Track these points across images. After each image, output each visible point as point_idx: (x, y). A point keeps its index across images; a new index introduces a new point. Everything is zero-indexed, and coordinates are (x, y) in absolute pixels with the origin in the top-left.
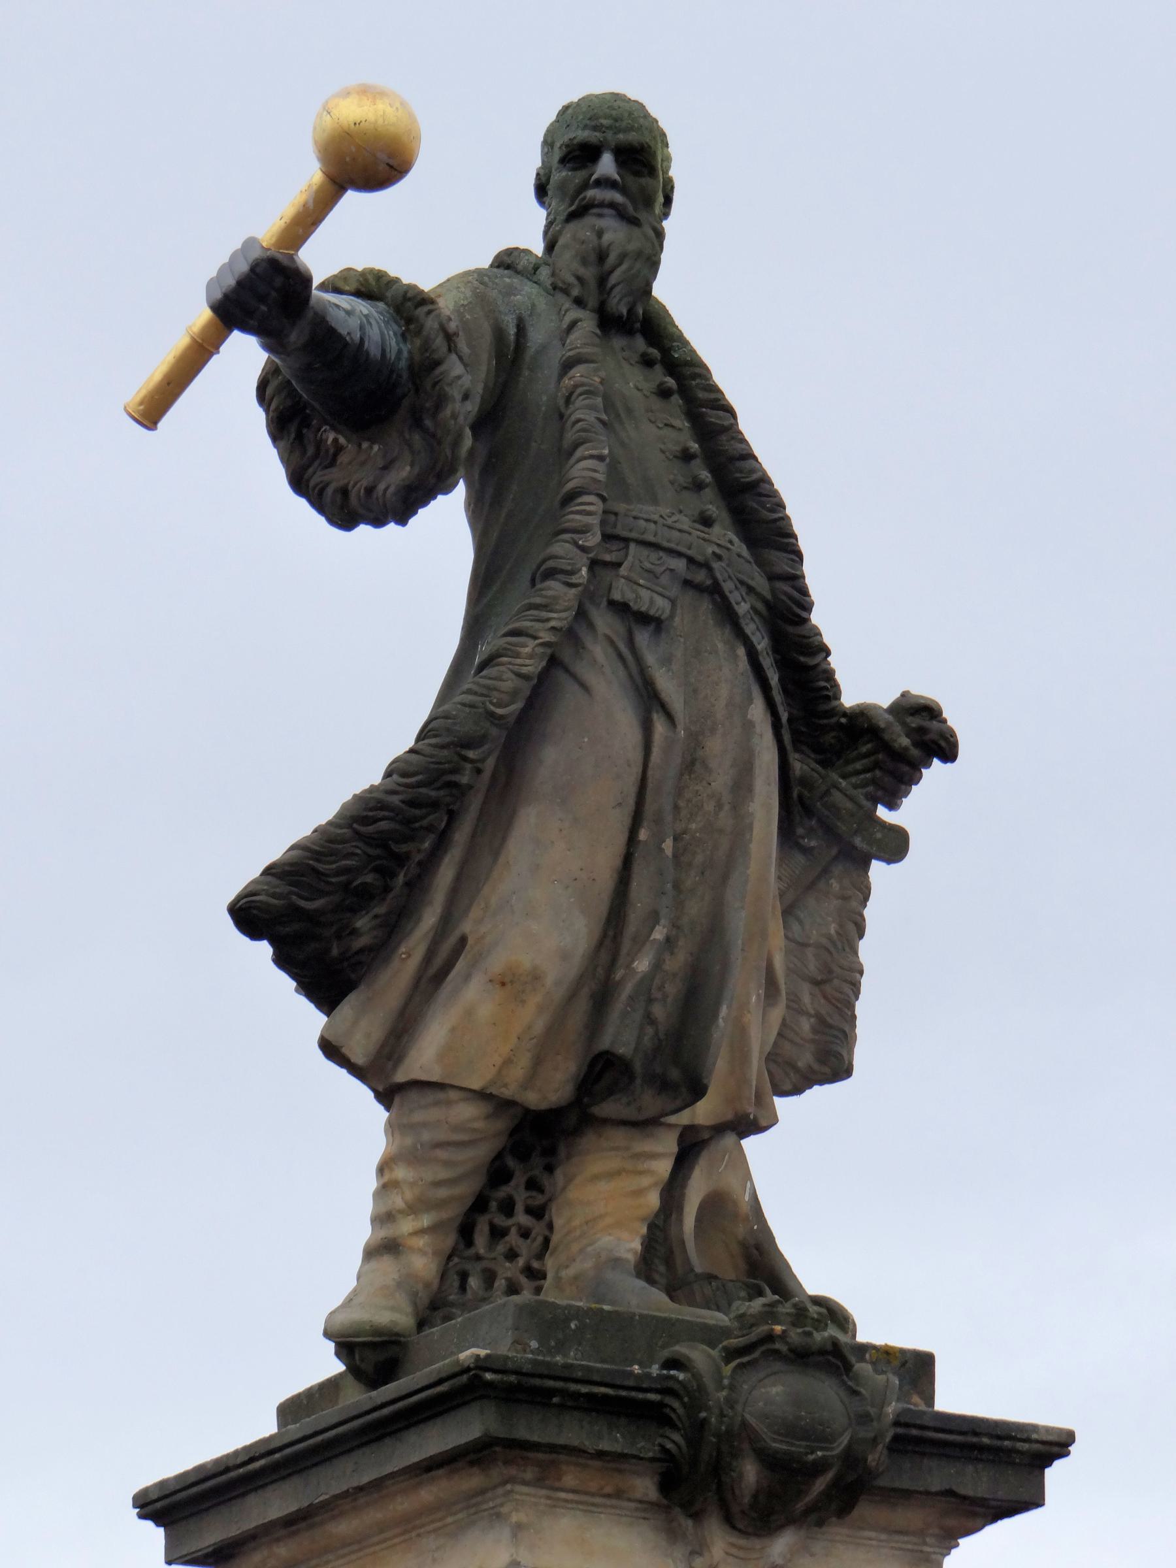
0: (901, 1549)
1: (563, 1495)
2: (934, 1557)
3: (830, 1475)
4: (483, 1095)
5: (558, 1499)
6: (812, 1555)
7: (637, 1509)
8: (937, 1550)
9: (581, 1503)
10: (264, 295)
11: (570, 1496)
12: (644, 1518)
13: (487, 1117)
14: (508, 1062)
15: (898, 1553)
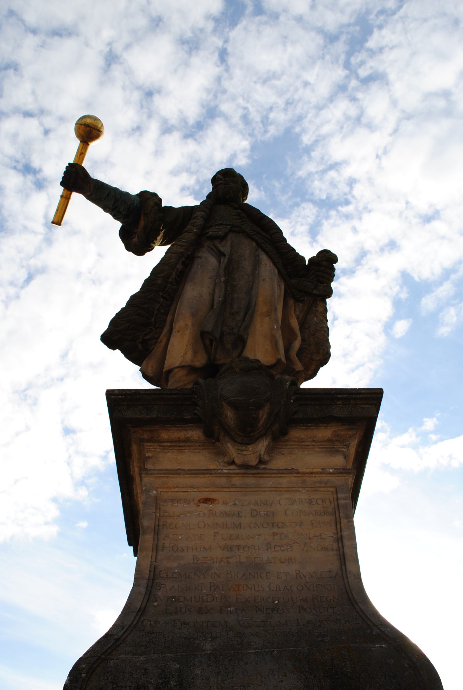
0: (324, 448)
1: (165, 444)
2: (341, 450)
3: (267, 409)
4: (181, 367)
5: (164, 446)
6: (283, 454)
7: (199, 446)
8: (341, 447)
9: (176, 446)
10: (75, 179)
11: (169, 444)
12: (204, 449)
13: (187, 375)
14: (185, 354)
15: (323, 450)
